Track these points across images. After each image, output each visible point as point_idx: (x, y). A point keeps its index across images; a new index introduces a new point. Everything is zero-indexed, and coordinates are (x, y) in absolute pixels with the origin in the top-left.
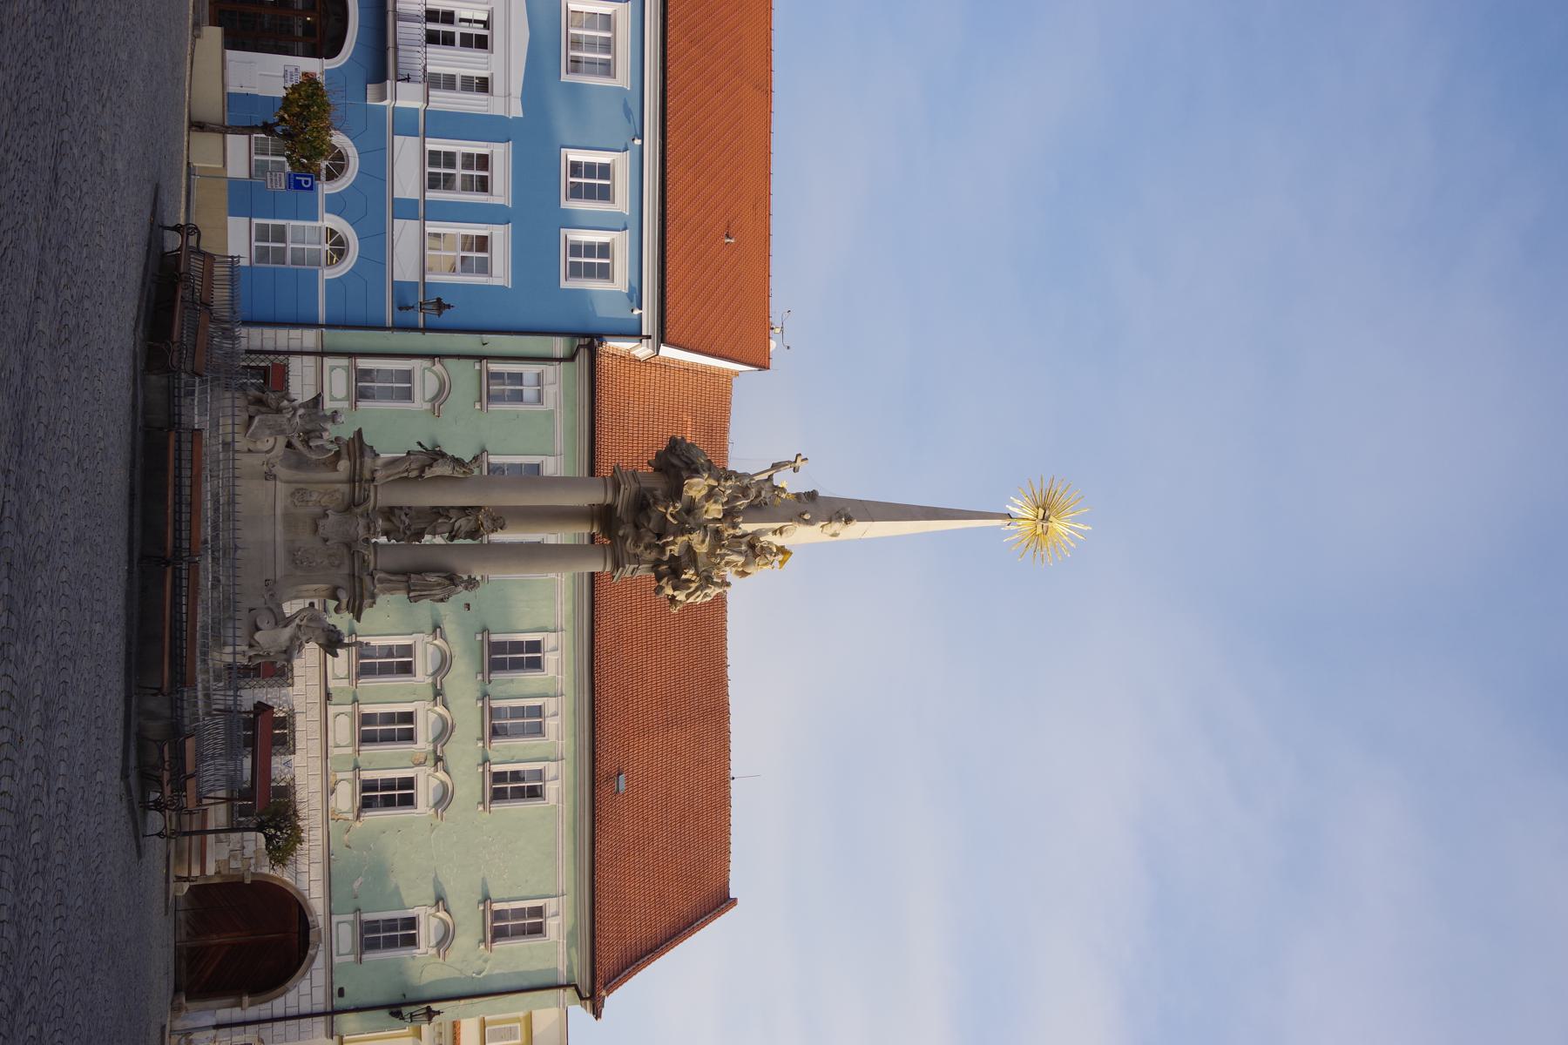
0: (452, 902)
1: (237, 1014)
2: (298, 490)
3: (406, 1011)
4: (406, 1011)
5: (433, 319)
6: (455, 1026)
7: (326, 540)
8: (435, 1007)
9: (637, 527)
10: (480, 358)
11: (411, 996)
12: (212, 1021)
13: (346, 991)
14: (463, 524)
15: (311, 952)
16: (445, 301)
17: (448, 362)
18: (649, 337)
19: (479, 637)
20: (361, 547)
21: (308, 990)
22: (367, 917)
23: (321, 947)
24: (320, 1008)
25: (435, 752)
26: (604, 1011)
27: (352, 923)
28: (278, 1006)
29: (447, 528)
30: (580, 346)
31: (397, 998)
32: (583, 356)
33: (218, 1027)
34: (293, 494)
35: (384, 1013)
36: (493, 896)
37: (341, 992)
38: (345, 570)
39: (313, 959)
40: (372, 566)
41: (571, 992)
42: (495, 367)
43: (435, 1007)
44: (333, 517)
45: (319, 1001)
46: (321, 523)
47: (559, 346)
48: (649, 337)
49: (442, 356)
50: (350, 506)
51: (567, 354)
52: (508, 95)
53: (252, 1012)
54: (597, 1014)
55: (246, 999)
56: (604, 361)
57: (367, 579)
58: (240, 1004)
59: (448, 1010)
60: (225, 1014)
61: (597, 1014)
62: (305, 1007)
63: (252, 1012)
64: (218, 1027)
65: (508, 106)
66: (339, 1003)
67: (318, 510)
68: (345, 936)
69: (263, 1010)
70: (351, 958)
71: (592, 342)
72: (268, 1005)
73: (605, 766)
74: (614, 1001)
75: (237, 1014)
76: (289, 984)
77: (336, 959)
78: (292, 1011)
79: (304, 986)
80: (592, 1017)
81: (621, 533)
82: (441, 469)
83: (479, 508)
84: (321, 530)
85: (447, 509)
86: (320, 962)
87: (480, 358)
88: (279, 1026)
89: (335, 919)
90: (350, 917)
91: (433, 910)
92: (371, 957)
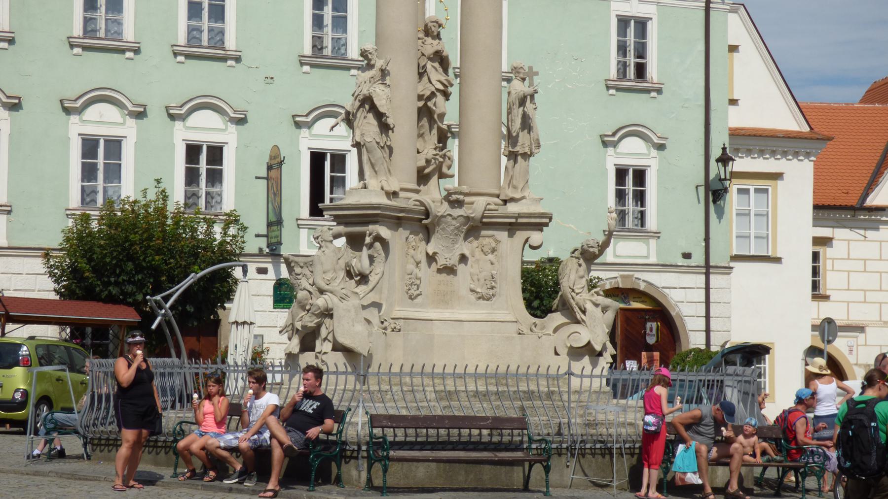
6: (735, 134)
7: (463, 259)
8: (716, 152)
13: (687, 251)
15: (642, 287)
19: (306, 68)
23: (637, 275)
29: (440, 98)
37: (687, 256)
38: (502, 235)
46: (441, 261)
59: (720, 139)
66: (698, 258)
70: (653, 242)
76: (673, 314)
77: (653, 260)
84: (449, 263)
92: (652, 223)
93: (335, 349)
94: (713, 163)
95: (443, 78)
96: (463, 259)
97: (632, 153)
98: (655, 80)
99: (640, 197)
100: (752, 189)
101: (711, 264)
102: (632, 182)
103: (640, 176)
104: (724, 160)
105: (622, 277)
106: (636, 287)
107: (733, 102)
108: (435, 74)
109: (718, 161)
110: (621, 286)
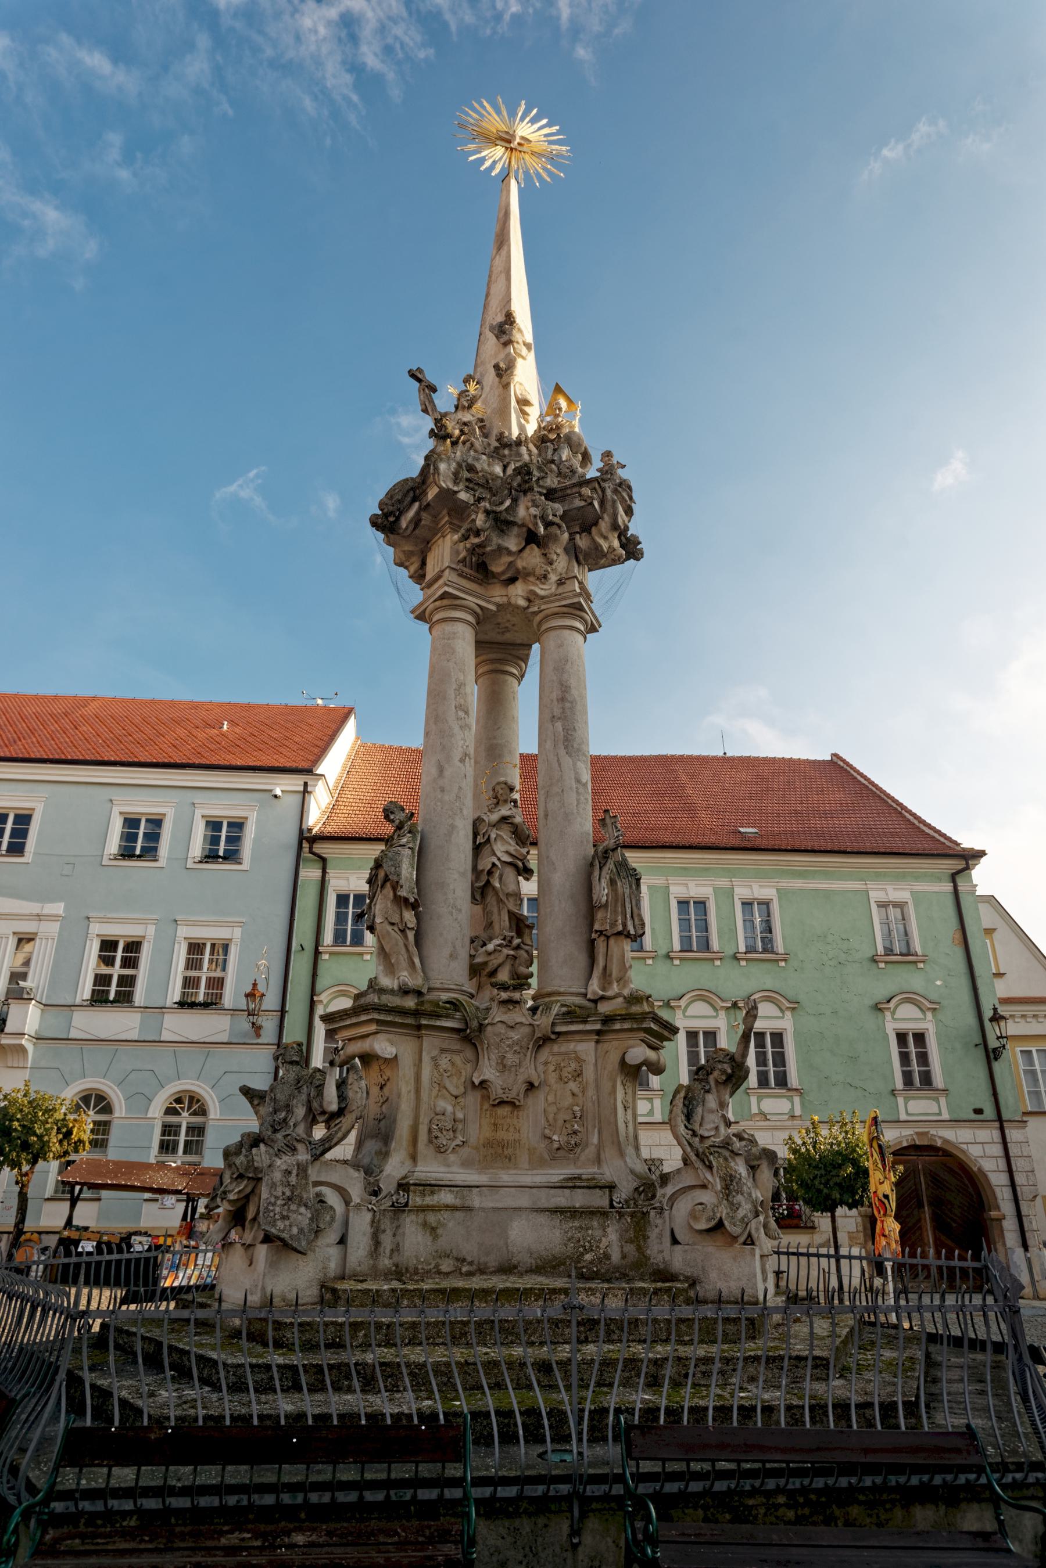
0: (881, 992)
1: (1010, 1225)
2: (432, 1139)
3: (993, 1043)
4: (993, 1043)
5: (271, 1001)
7: (531, 1086)
8: (988, 1013)
9: (512, 580)
10: (317, 953)
11: (978, 1040)
12: (1020, 1251)
13: (978, 1106)
14: (503, 847)
15: (939, 1143)
16: (249, 989)
17: (319, 987)
18: (306, 784)
20: (543, 1021)
21: (978, 1146)
22: (899, 1084)
23: (933, 1132)
24: (996, 1134)
25: (728, 1008)
26: (978, 847)
27: (907, 1100)
28: (998, 1180)
29: (510, 873)
30: (311, 852)
31: (980, 1053)
32: (320, 848)
33: (1025, 1247)
34: (440, 1150)
35: (996, 1066)
36: (870, 954)
37: (979, 1111)
38: (586, 1048)
39: (946, 1141)
40: (579, 1000)
41: (960, 880)
42: (328, 937)
43: (988, 1013)
44: (488, 1072)
45: (989, 1134)
47: (310, 874)
48: (306, 784)
49: (313, 992)
50: (471, 1036)
51: (320, 865)
52: (39, 917)
53: (1007, 1207)
54: (982, 854)
55: (993, 1214)
56: (330, 830)
57: (604, 1008)
58: (1000, 1220)
60: (1011, 1238)
61: (982, 854)
62: (997, 1150)
63: (1007, 1207)
64: (1025, 1247)
65: (53, 918)
66: (989, 1112)
67: (473, 1099)
68: (920, 1107)
69: (1003, 1195)
70: (943, 1100)
71: (308, 839)
72: (997, 1190)
73: (735, 842)
74: (967, 841)
75: (1010, 1225)
76: (975, 1169)
77: (946, 1116)
78: (1002, 1164)
79: (975, 1151)
80: (983, 860)
81: (522, 603)
82: (407, 871)
83: (477, 823)
85: (476, 871)
86: (949, 1134)
87: (317, 953)
88: (1020, 1179)
89: (903, 1117)
90: (900, 1100)
91: (888, 1014)
92: (939, 1080)
93: (268, 1239)
94: (987, 1024)
95: (513, 847)
96: (531, 1086)
97: (907, 1017)
98: (920, 953)
99: (923, 1058)
100: (1034, 1050)
101: (1005, 1117)
102: (912, 1043)
103: (920, 1038)
104: (996, 1018)
105: (917, 1133)
106: (933, 1143)
107: (999, 975)
108: (503, 847)
109: (991, 1020)
110: (918, 1143)
